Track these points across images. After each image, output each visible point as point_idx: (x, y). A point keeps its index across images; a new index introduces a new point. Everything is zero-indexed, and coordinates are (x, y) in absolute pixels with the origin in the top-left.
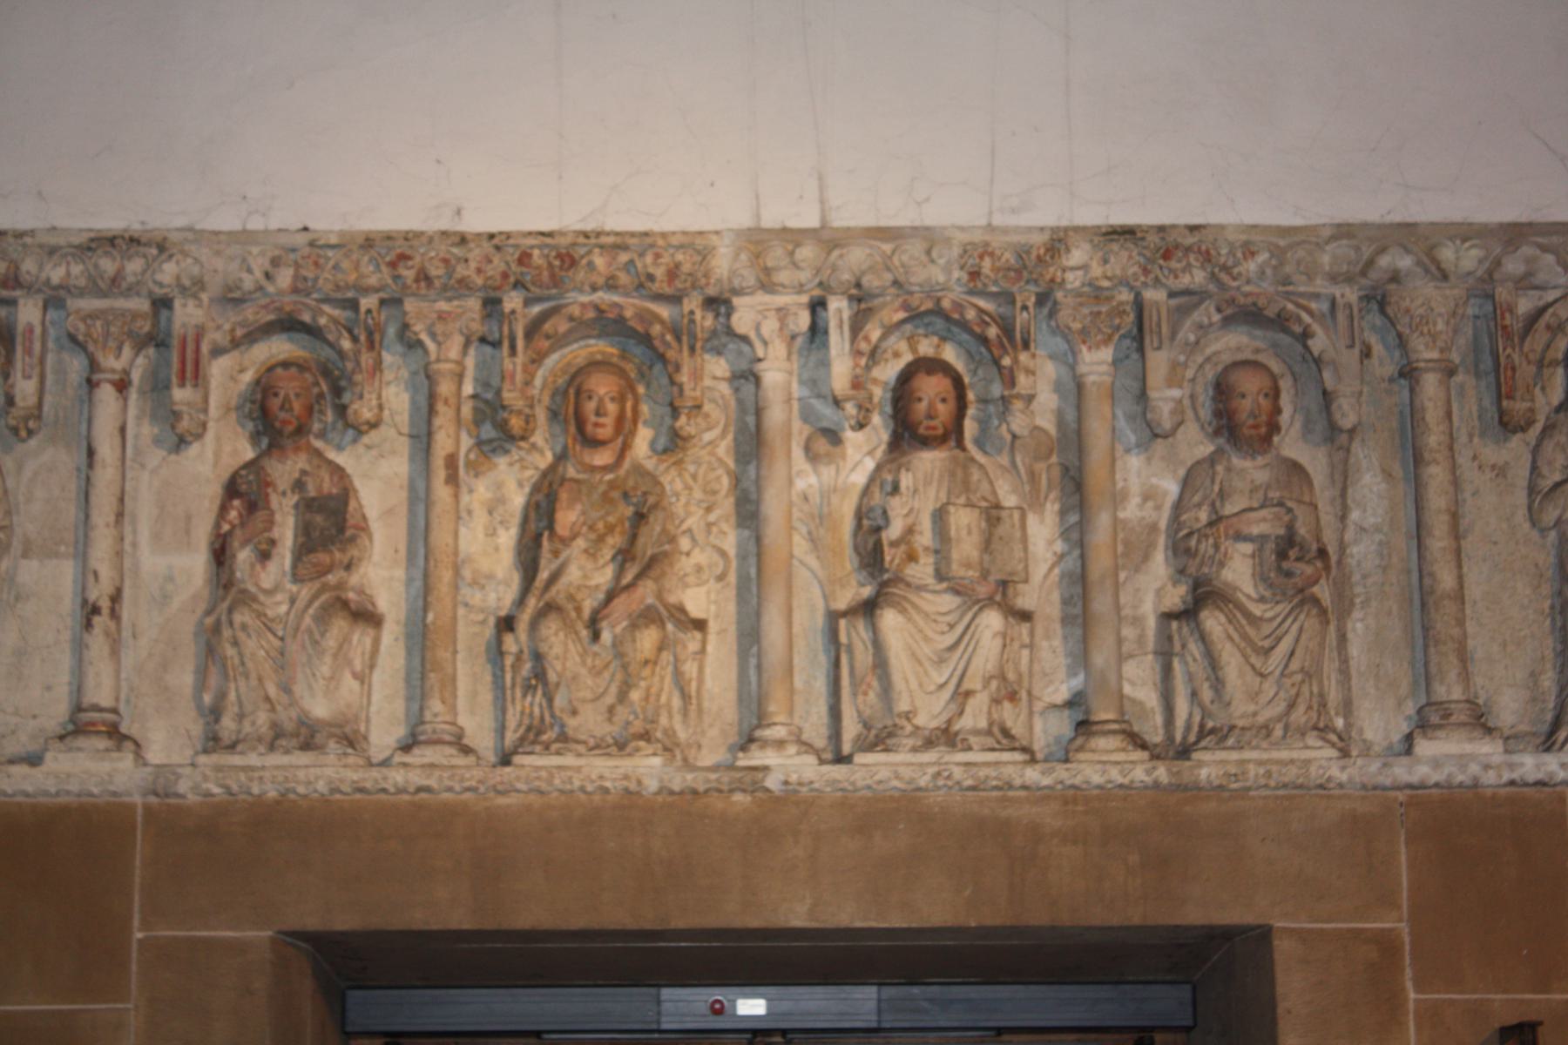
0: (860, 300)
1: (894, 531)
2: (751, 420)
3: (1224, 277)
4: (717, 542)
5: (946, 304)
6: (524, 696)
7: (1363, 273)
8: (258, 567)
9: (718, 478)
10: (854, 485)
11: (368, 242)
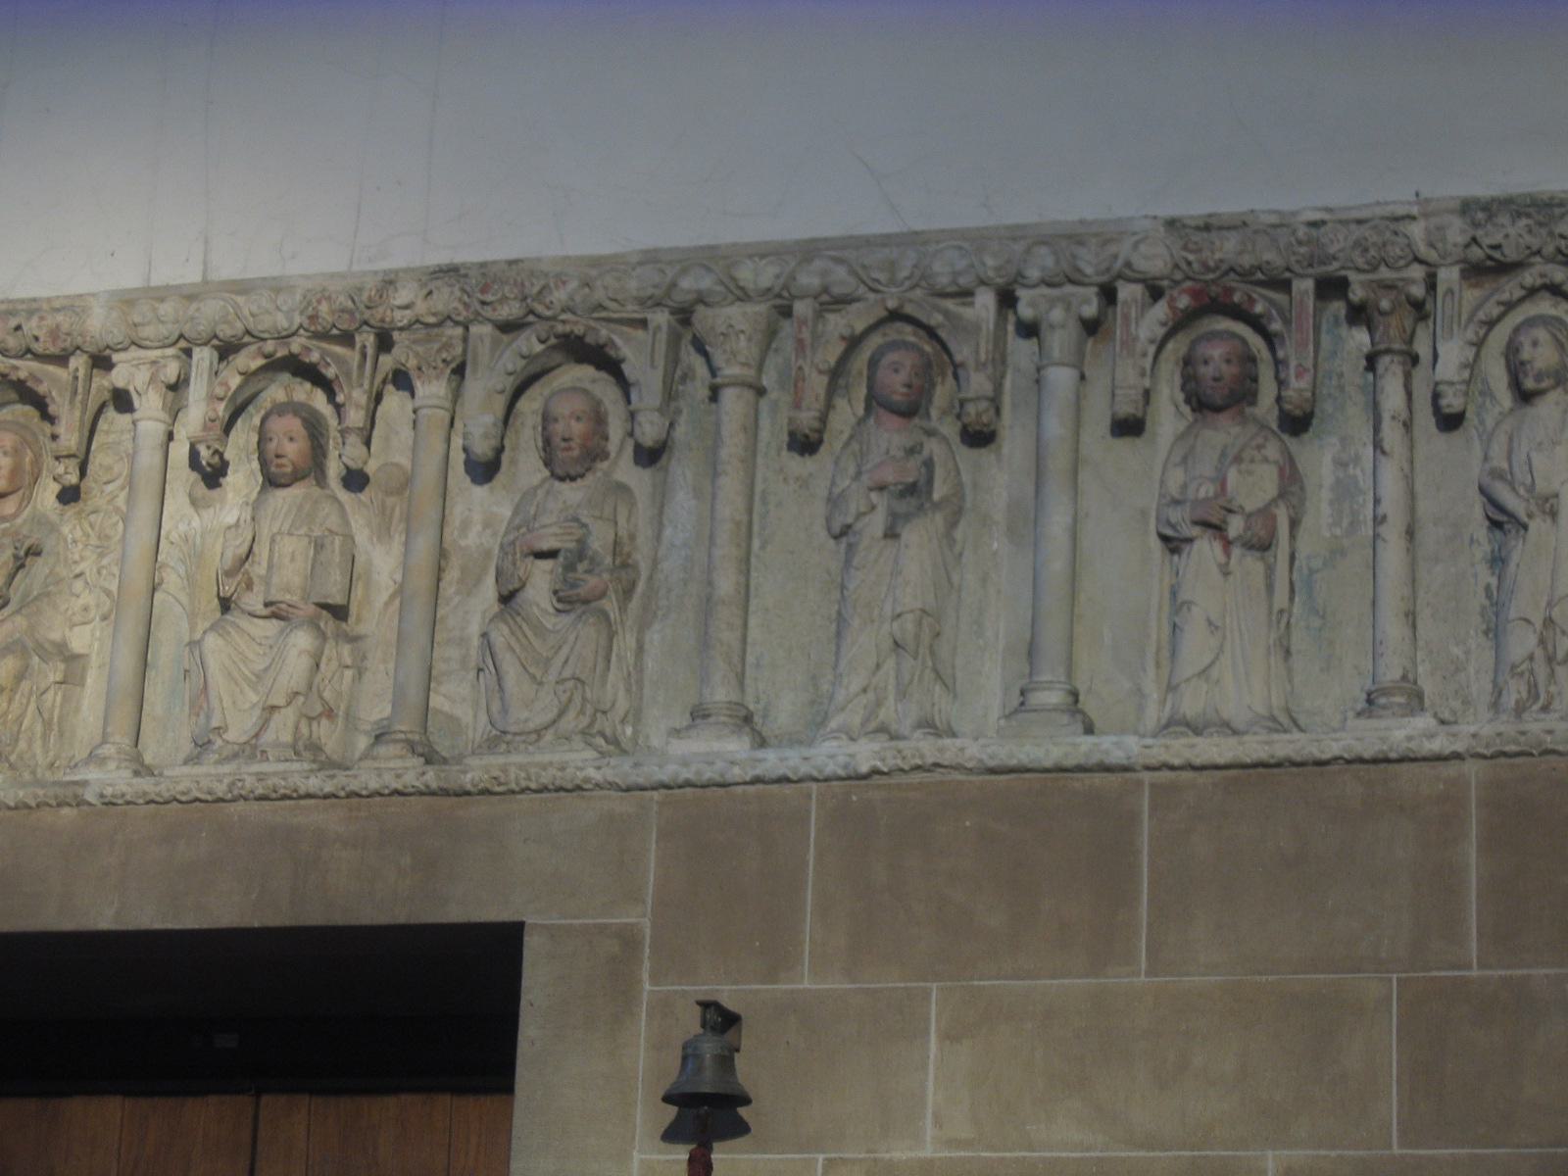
3: (540, 309)
4: (106, 585)
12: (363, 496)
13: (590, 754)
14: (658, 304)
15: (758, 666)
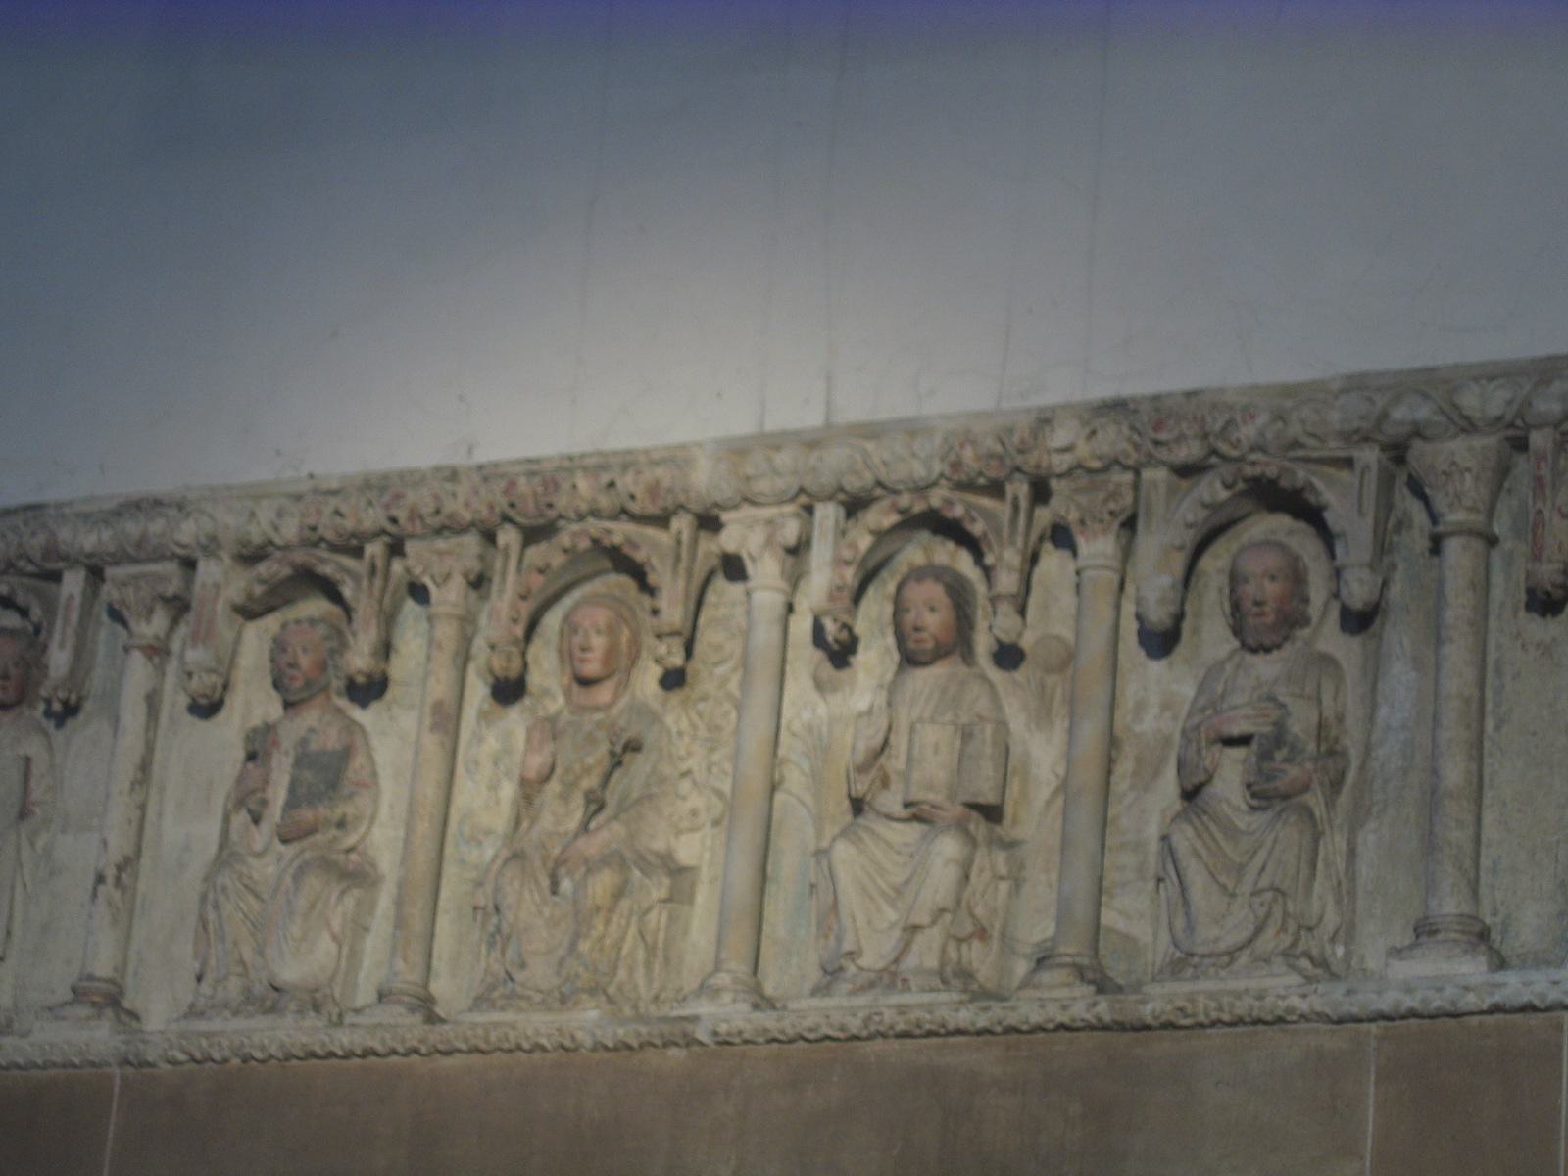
3: (1223, 447)
8: (253, 828)
9: (726, 714)
12: (1019, 675)
13: (1294, 979)
14: (1366, 439)
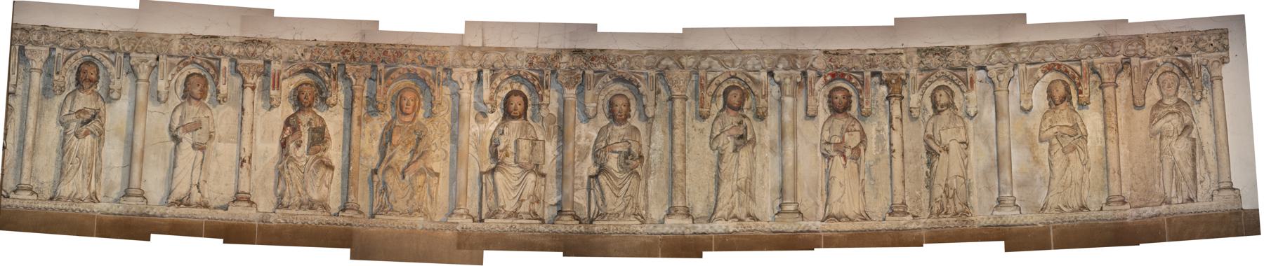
0: (494, 71)
1: (501, 147)
2: (457, 108)
5: (522, 73)
6: (380, 196)
7: (657, 66)
10: (490, 131)
11: (336, 45)
15: (689, 192)
